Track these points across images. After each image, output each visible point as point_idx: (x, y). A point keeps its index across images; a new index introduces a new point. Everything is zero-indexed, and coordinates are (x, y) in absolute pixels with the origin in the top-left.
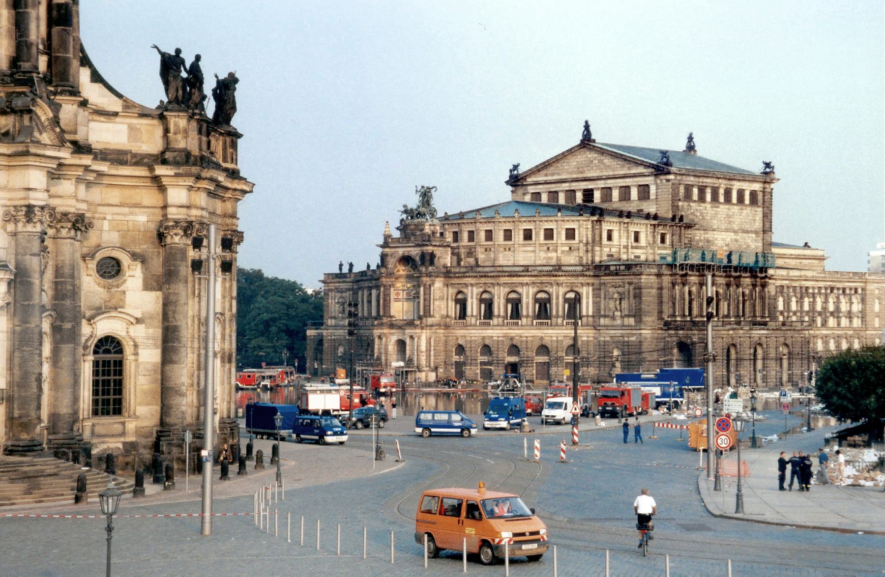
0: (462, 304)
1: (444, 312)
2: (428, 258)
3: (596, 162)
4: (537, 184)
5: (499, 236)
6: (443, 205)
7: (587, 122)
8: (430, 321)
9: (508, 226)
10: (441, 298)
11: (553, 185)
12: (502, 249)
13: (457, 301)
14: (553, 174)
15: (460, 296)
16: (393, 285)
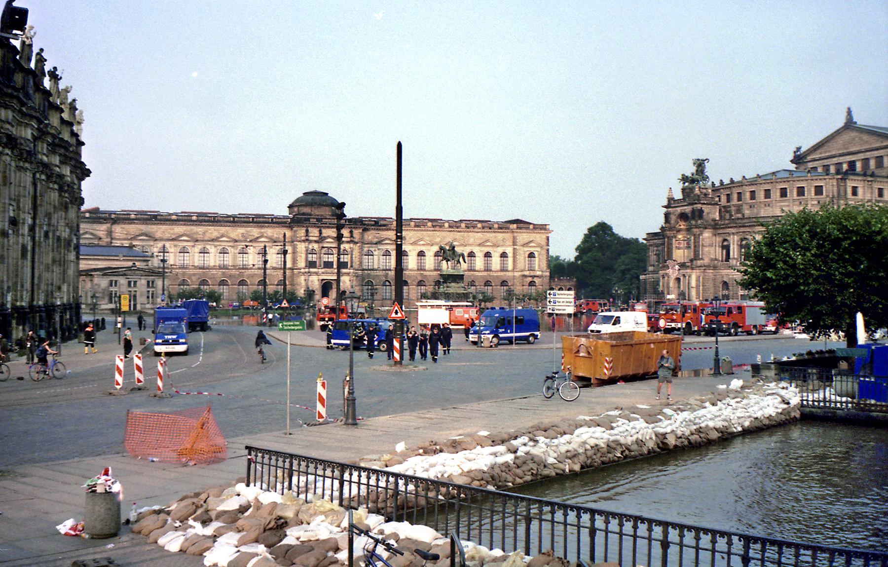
0: (727, 248)
1: (713, 257)
2: (697, 213)
3: (857, 139)
4: (814, 160)
5: (761, 195)
6: (716, 174)
7: (849, 109)
8: (699, 263)
9: (767, 187)
10: (711, 245)
11: (825, 161)
12: (763, 206)
13: (723, 247)
14: (825, 152)
15: (725, 243)
16: (675, 237)
